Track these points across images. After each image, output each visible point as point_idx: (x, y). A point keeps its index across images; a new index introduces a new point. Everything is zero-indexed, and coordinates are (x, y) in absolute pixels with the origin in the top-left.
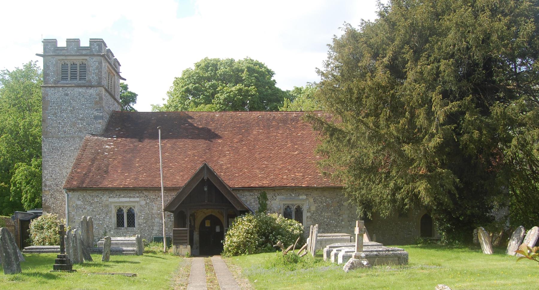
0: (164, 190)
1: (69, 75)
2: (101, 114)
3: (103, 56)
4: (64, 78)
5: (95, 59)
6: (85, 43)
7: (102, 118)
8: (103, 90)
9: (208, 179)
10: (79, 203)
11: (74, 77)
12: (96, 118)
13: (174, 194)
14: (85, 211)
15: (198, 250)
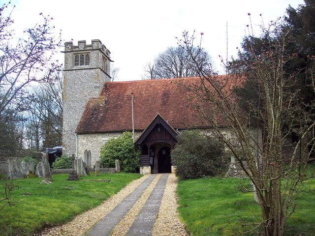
0: (135, 131)
1: (79, 62)
2: (98, 85)
3: (100, 50)
4: (76, 65)
5: (94, 52)
6: (89, 43)
7: (98, 87)
8: (100, 70)
9: (160, 124)
10: (84, 141)
11: (82, 64)
12: (96, 87)
13: (140, 134)
14: (87, 146)
15: (157, 170)
